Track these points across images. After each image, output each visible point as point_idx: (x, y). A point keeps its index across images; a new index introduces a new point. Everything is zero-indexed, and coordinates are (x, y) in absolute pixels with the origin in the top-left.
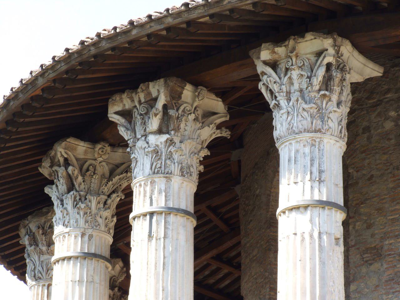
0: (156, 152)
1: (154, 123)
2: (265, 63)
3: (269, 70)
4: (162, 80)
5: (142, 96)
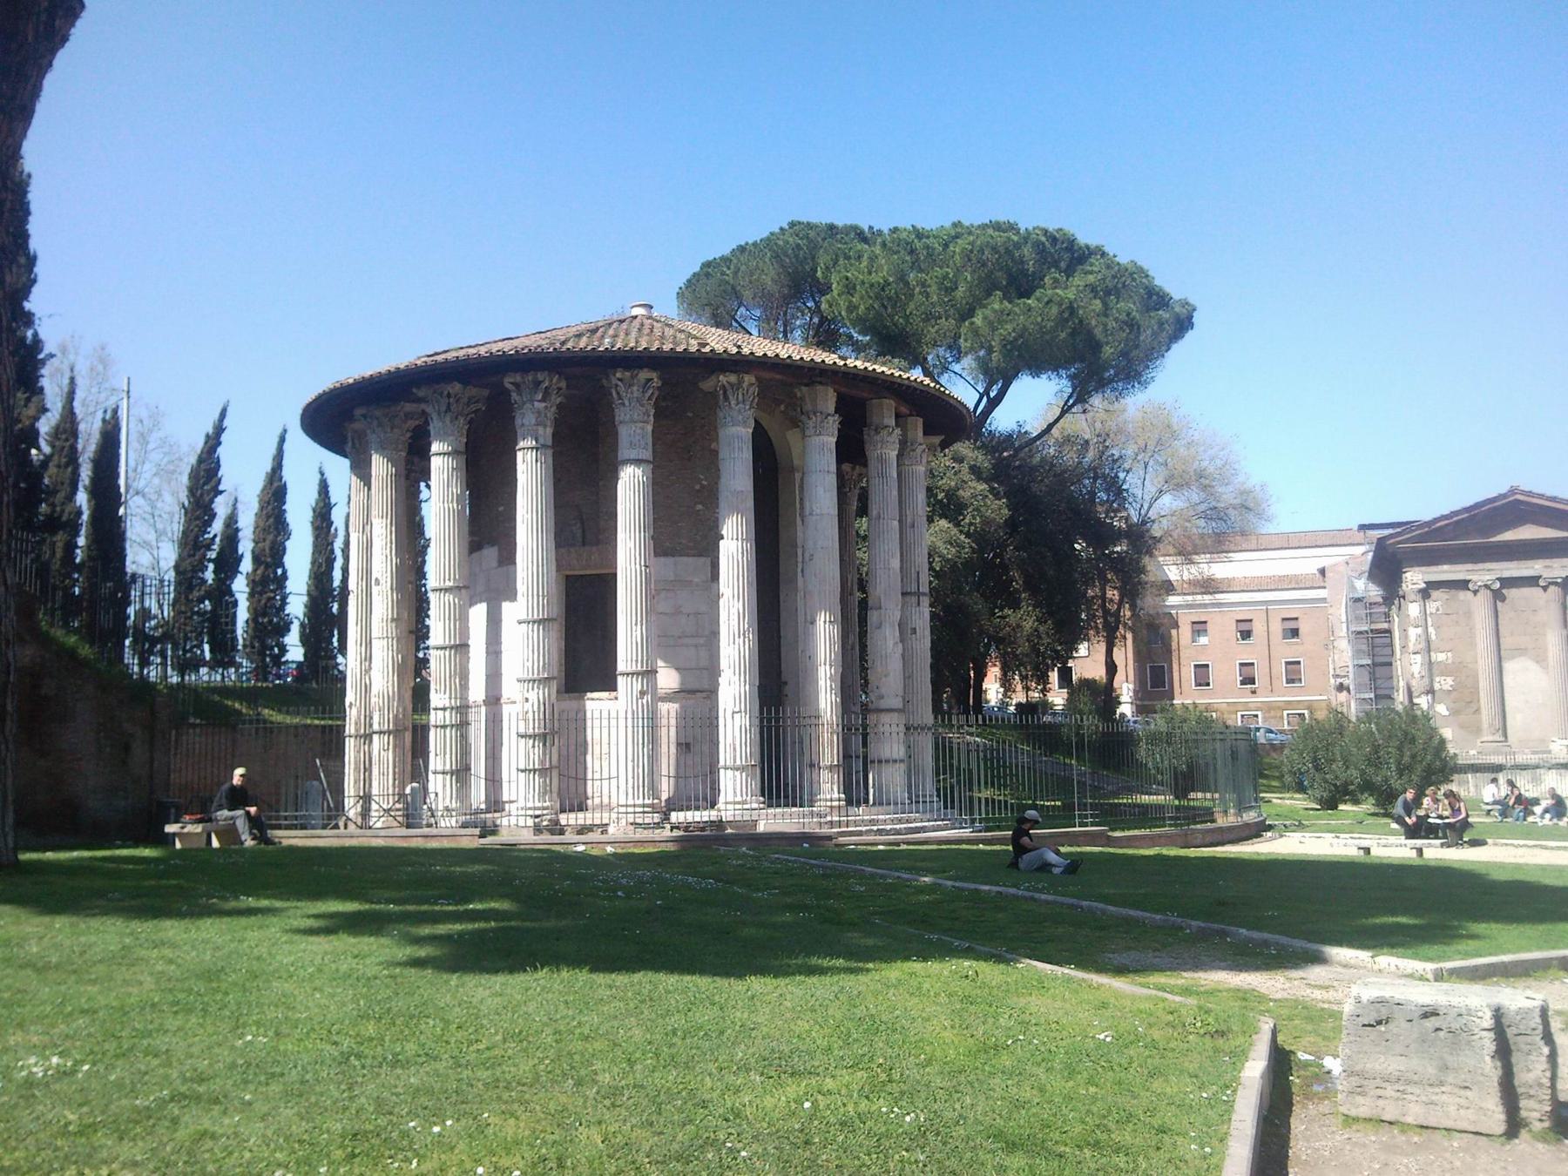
0: (539, 412)
1: (540, 397)
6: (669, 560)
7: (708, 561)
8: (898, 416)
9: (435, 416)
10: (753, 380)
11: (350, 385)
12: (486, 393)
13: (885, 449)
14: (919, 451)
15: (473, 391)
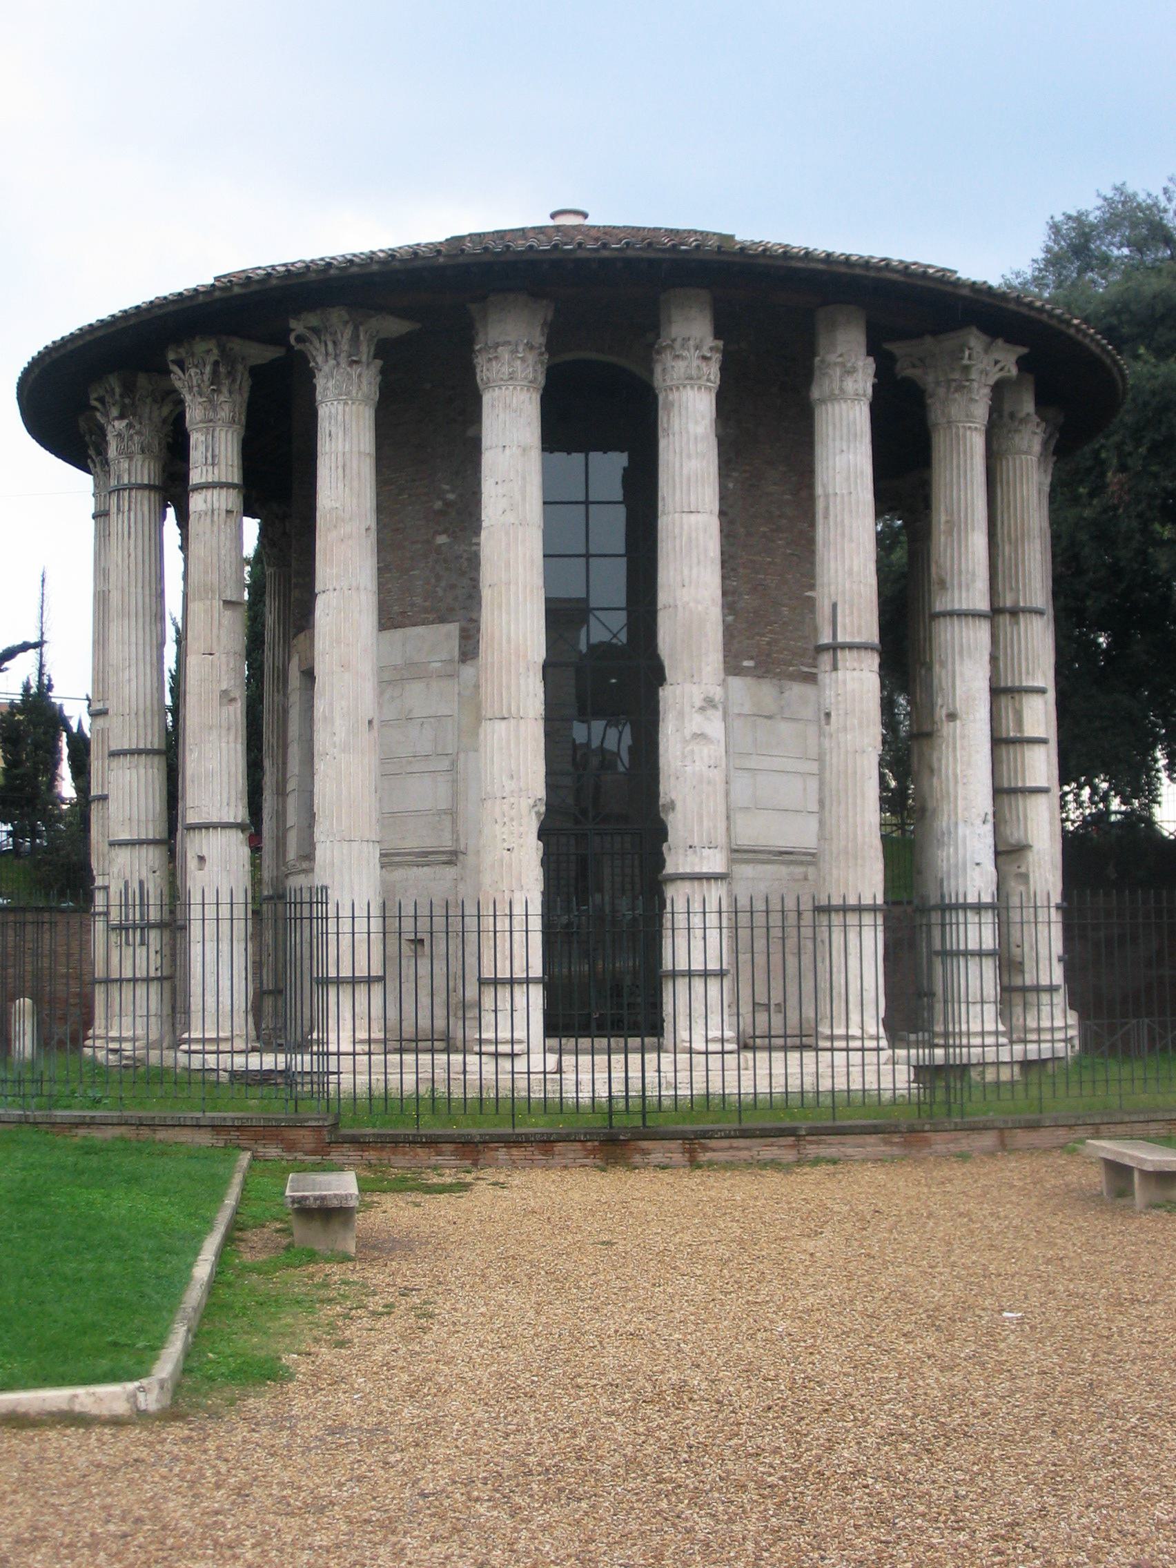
1: (115, 412)
2: (173, 361)
3: (175, 368)
6: (399, 633)
7: (453, 628)
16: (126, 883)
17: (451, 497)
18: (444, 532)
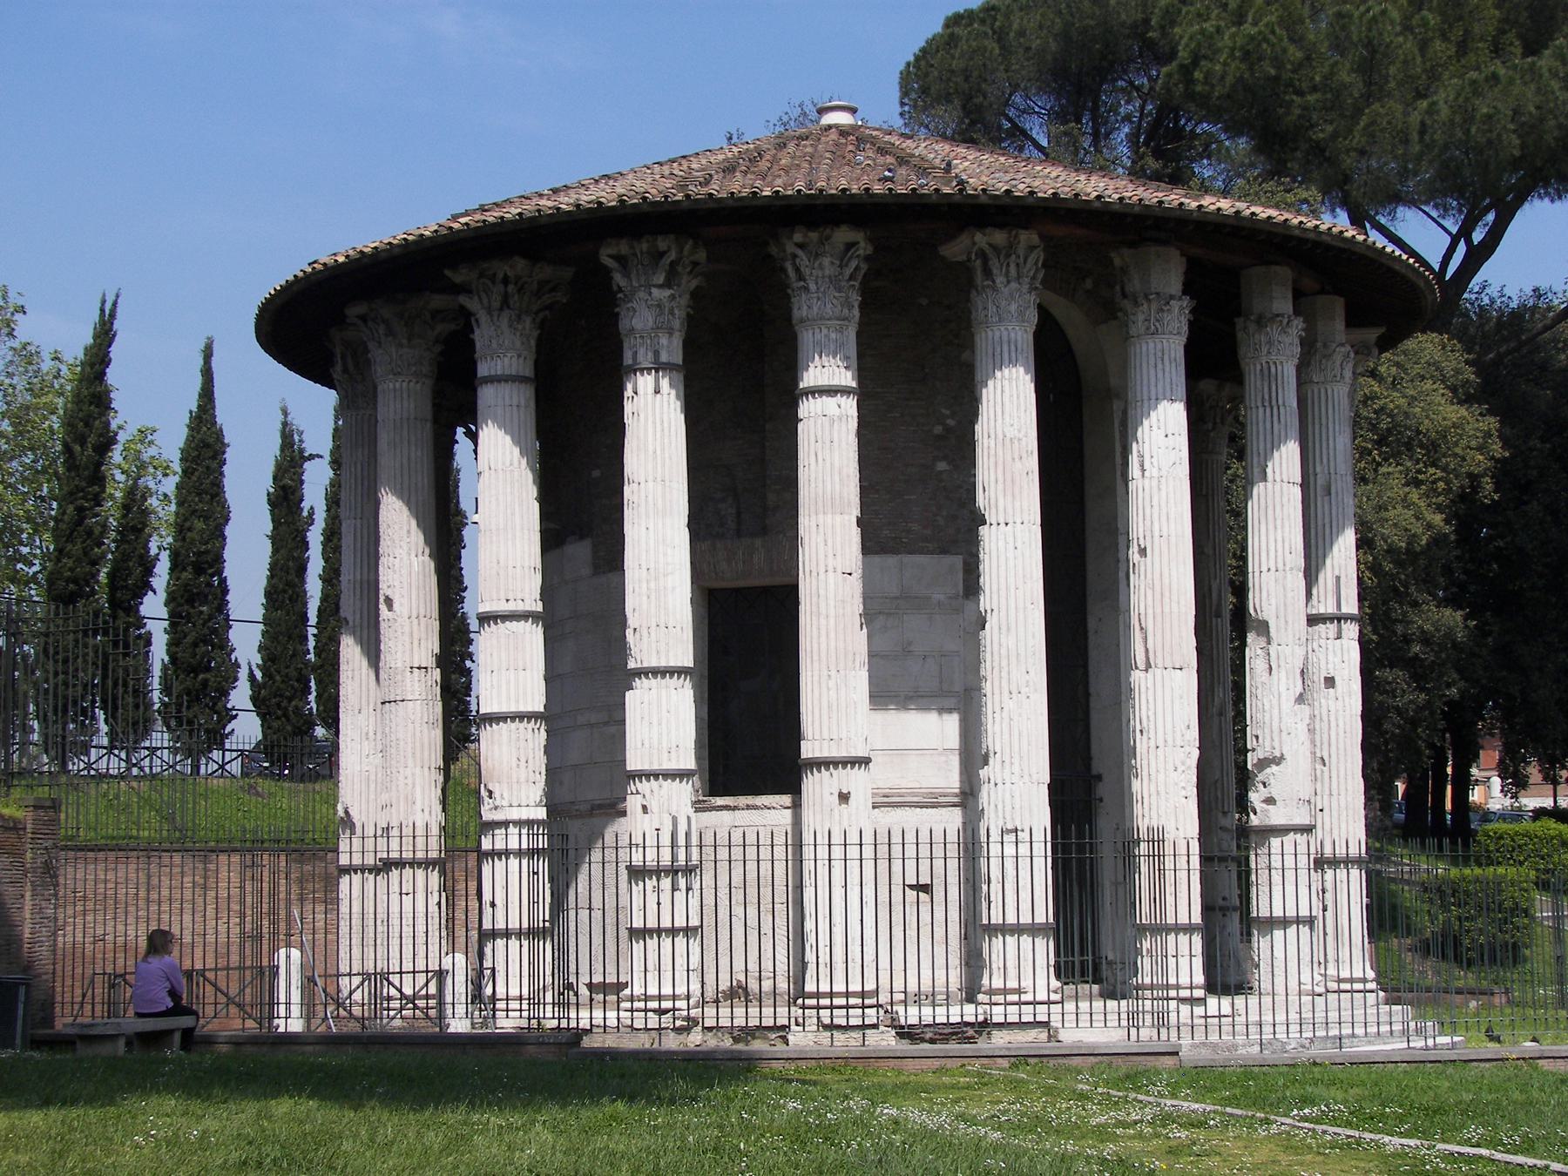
0: (659, 306)
3: (800, 252)
4: (672, 237)
5: (645, 246)
6: (891, 560)
7: (957, 561)
8: (1298, 295)
9: (483, 317)
10: (1035, 239)
11: (338, 265)
12: (568, 273)
13: (1275, 357)
14: (1338, 358)
15: (545, 272)
16: (675, 820)
17: (951, 422)
18: (945, 458)
